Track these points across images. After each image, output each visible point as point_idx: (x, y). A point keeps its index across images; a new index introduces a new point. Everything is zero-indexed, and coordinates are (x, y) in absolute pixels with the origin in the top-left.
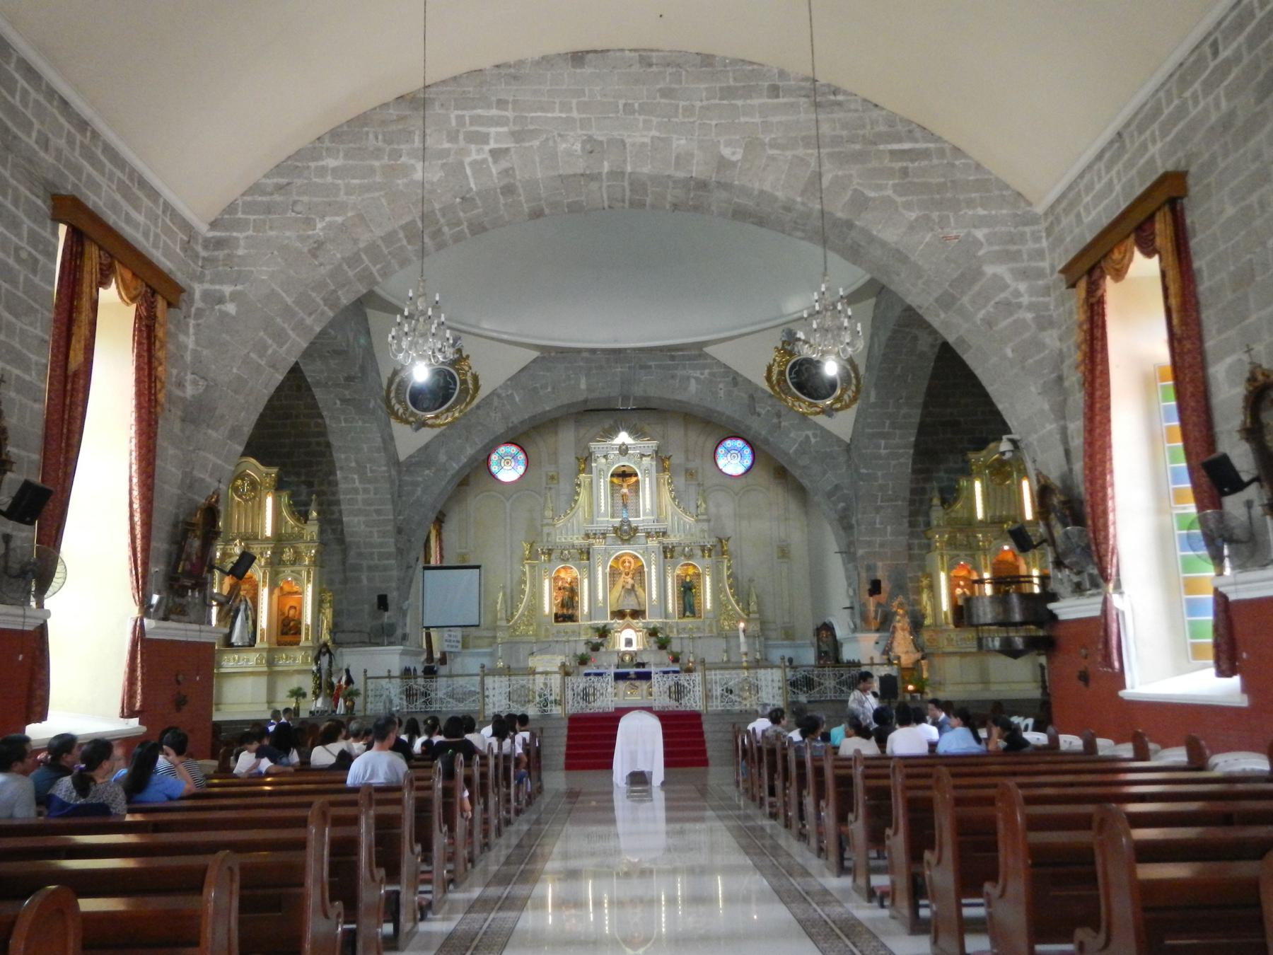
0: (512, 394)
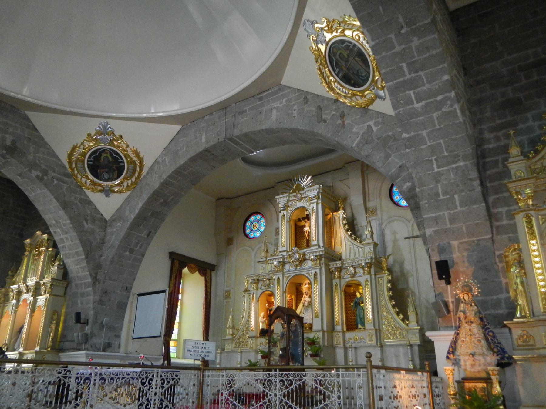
0: (165, 159)
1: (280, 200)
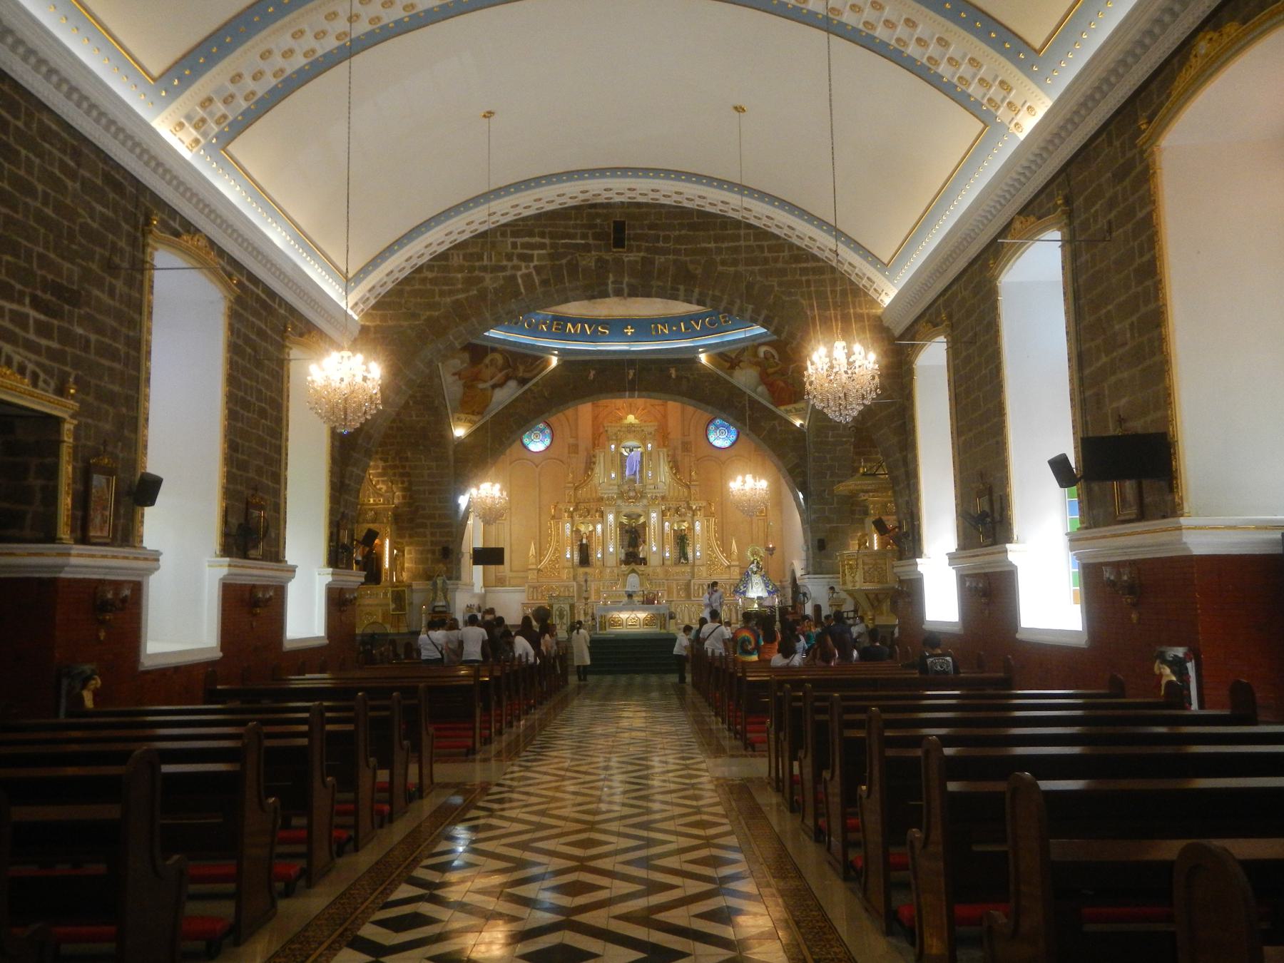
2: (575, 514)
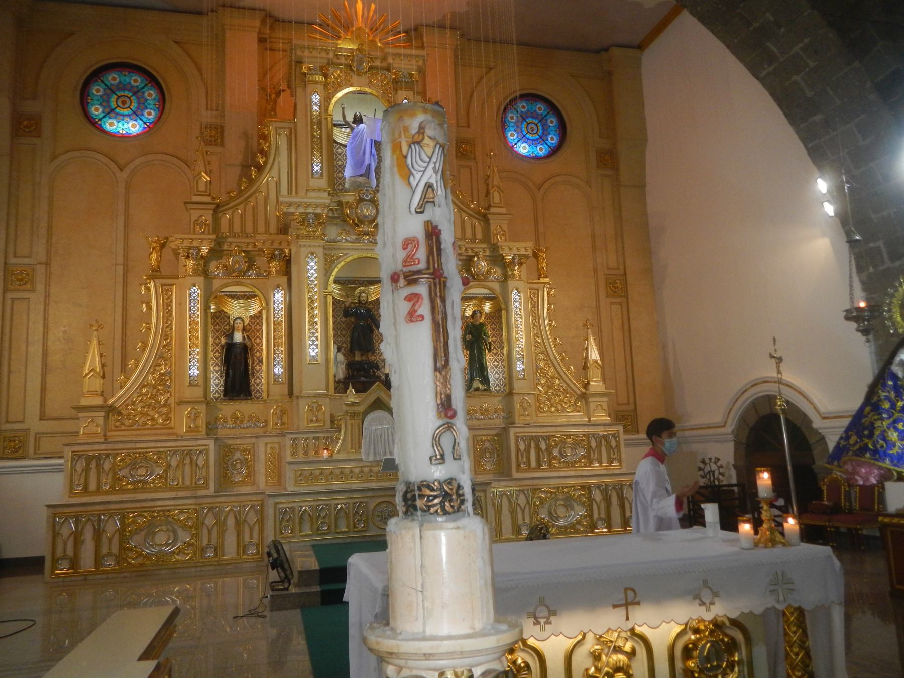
1: (307, 53)
2: (213, 265)
